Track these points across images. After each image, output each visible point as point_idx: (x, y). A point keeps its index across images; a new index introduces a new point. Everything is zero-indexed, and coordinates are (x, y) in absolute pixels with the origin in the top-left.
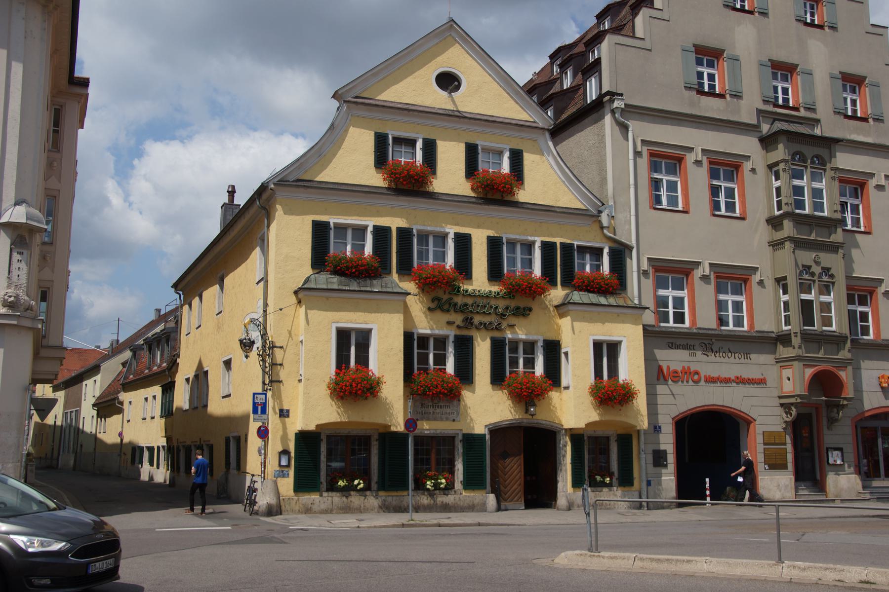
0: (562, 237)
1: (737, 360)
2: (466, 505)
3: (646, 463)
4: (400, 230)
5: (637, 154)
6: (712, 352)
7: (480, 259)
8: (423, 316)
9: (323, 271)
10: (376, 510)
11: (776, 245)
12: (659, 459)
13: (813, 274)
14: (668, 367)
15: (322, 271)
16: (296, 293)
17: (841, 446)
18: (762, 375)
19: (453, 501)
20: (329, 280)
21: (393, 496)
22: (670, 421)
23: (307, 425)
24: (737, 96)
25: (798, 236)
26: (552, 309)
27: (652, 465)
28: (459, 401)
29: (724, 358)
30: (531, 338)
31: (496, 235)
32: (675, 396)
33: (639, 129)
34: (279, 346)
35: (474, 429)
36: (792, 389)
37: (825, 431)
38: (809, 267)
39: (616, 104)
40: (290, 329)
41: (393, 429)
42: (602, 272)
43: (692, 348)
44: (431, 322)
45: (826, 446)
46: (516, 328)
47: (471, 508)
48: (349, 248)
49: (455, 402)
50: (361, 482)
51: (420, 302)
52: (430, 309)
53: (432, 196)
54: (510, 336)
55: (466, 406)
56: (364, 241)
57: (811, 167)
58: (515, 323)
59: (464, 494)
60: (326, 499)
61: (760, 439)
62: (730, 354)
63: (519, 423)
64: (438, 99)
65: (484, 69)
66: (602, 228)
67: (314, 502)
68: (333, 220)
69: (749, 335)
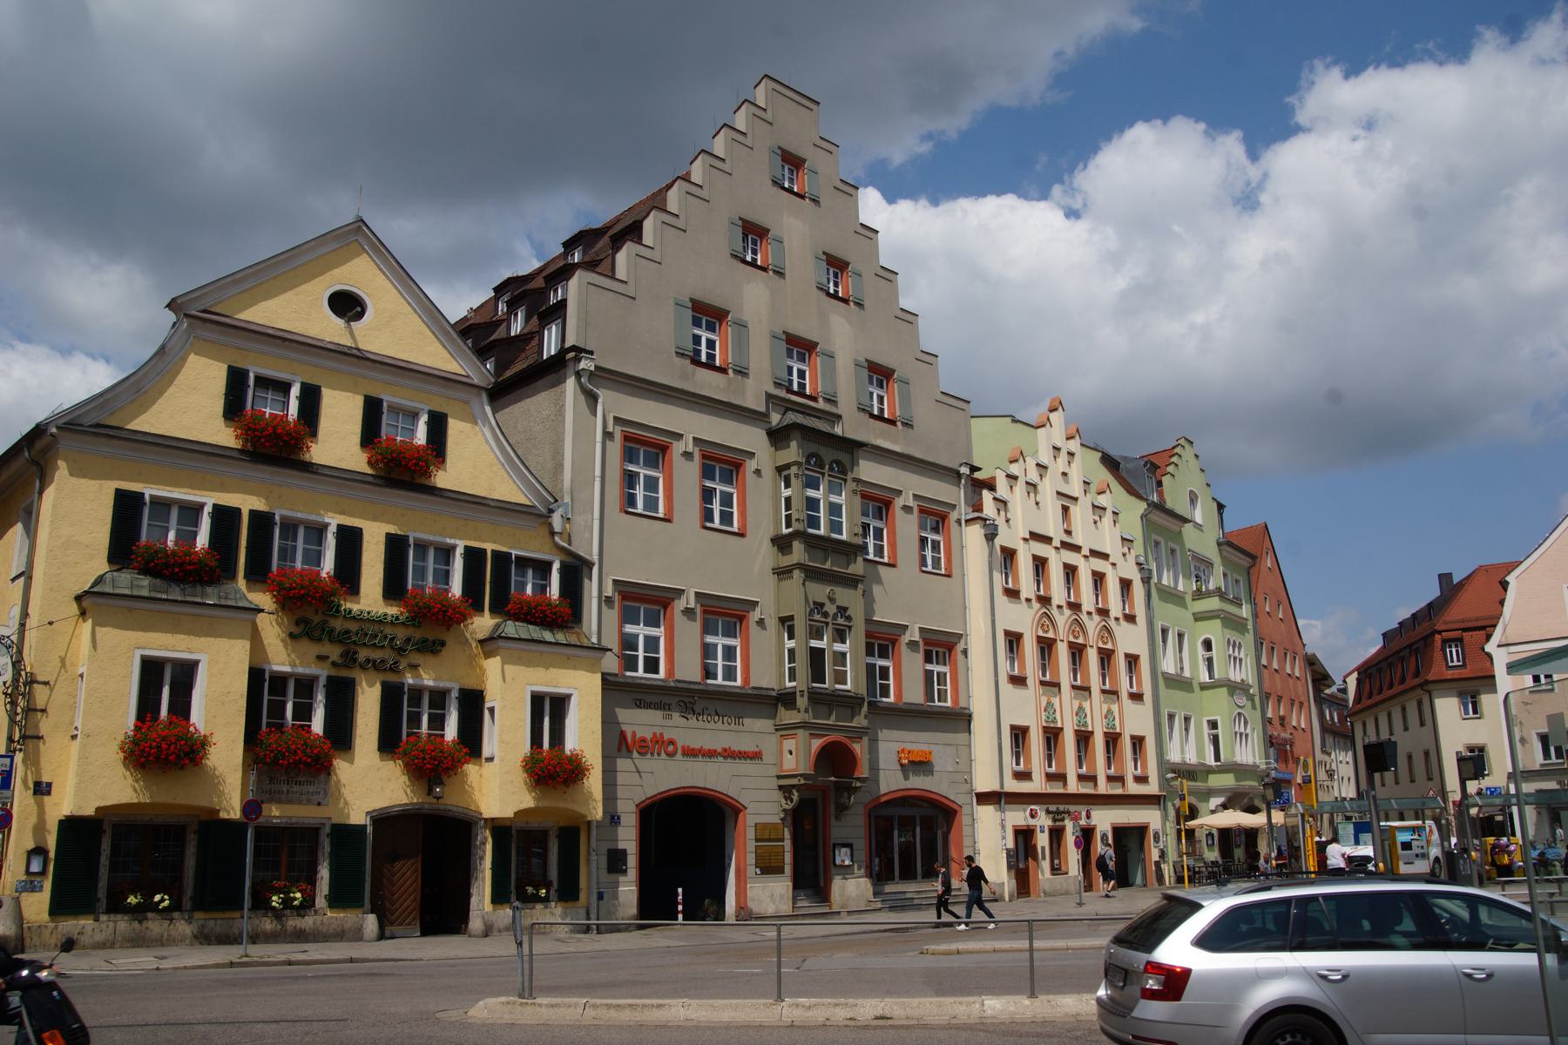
0: (494, 542)
1: (726, 726)
2: (331, 931)
3: (598, 868)
4: (253, 513)
5: (608, 435)
7: (373, 566)
8: (281, 644)
9: (127, 568)
10: (188, 941)
11: (782, 573)
12: (616, 861)
13: (826, 615)
14: (634, 734)
15: (124, 568)
16: (78, 598)
17: (850, 841)
18: (757, 746)
19: (312, 927)
20: (135, 583)
21: (216, 919)
22: (634, 809)
23: (80, 808)
24: (742, 372)
25: (811, 564)
26: (474, 645)
27: (606, 871)
28: (329, 774)
29: (709, 722)
30: (441, 685)
31: (399, 533)
32: (642, 774)
33: (612, 402)
34: (42, 680)
35: (348, 816)
36: (794, 767)
37: (833, 822)
38: (822, 605)
39: (583, 365)
40: (63, 654)
41: (223, 815)
42: (548, 595)
43: (667, 708)
44: (293, 656)
45: (833, 841)
46: (421, 670)
47: (339, 935)
48: (171, 536)
49: (323, 777)
50: (166, 897)
51: (278, 624)
52: (291, 635)
53: (309, 468)
54: (410, 681)
55: (339, 781)
56: (197, 527)
57: (829, 475)
58: (419, 662)
59: (329, 914)
60: (104, 926)
61: (751, 834)
62: (717, 718)
63: (417, 809)
64: (330, 328)
65: (401, 294)
66: (553, 533)
67: (84, 930)
68: (149, 491)
69: (743, 691)
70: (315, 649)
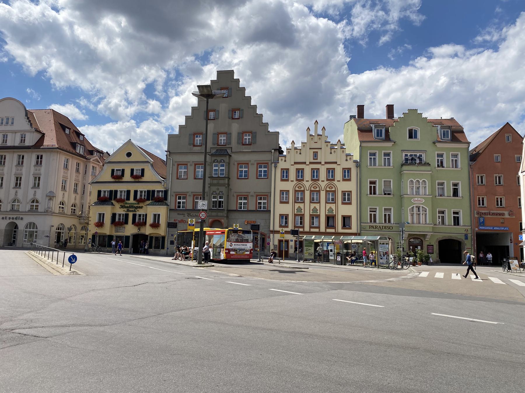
70: (122, 209)
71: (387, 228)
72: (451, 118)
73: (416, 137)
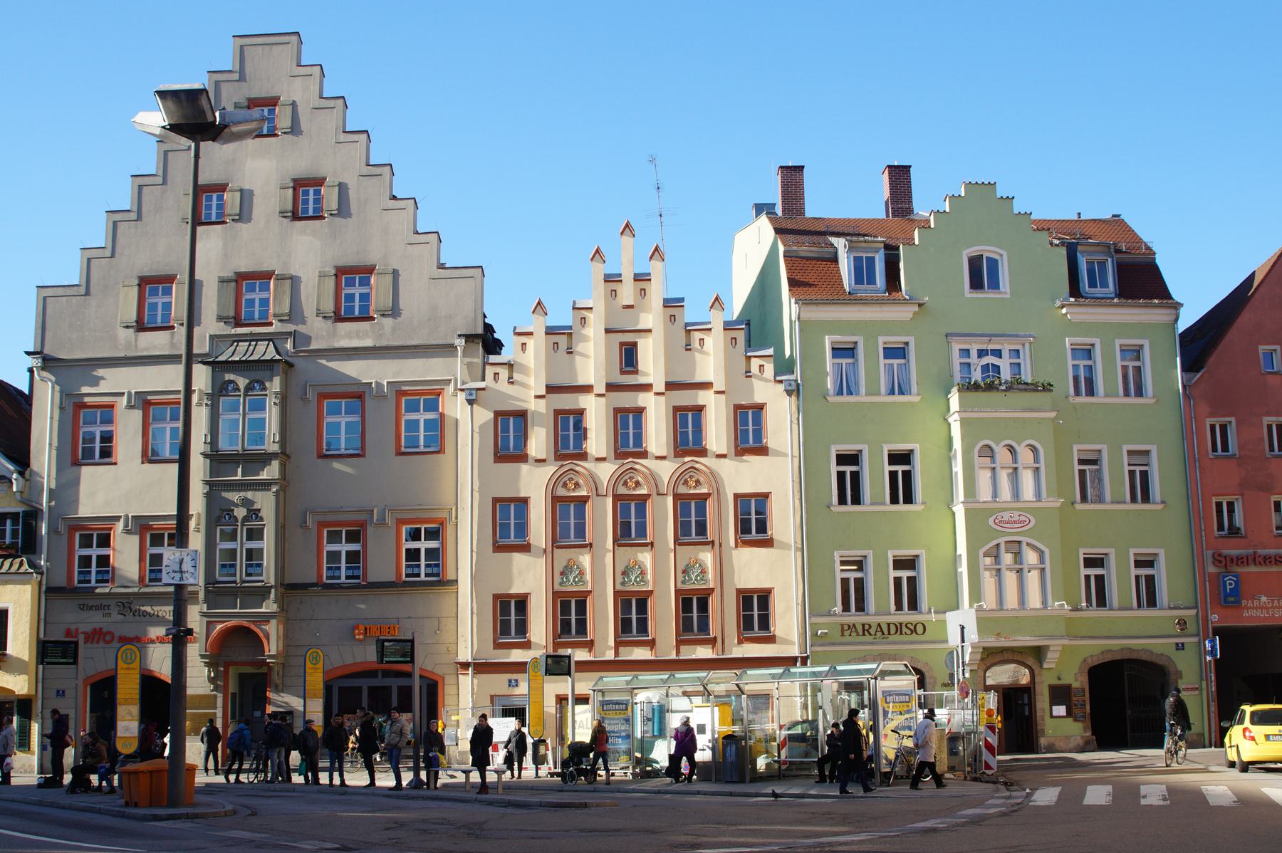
6: (131, 612)
71: (905, 630)
72: (1114, 216)
73: (995, 285)
